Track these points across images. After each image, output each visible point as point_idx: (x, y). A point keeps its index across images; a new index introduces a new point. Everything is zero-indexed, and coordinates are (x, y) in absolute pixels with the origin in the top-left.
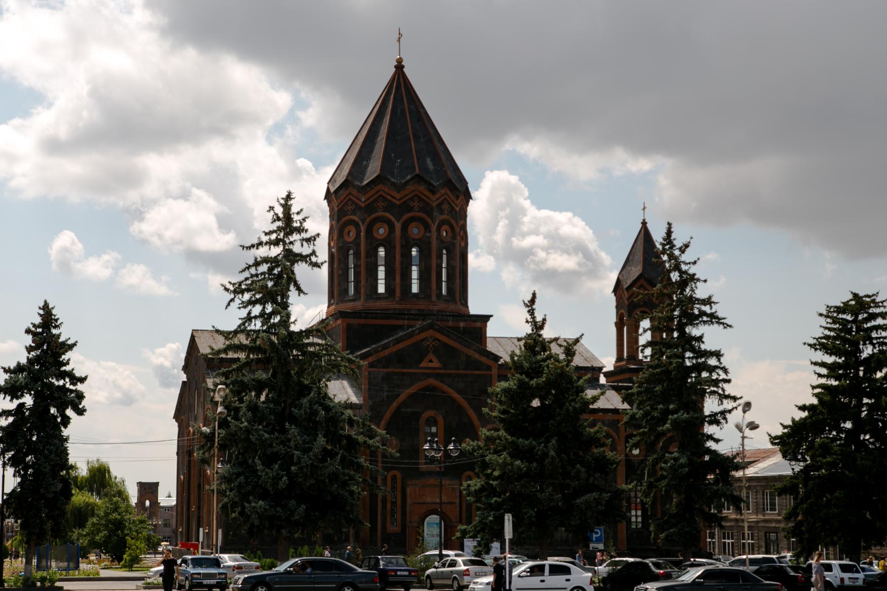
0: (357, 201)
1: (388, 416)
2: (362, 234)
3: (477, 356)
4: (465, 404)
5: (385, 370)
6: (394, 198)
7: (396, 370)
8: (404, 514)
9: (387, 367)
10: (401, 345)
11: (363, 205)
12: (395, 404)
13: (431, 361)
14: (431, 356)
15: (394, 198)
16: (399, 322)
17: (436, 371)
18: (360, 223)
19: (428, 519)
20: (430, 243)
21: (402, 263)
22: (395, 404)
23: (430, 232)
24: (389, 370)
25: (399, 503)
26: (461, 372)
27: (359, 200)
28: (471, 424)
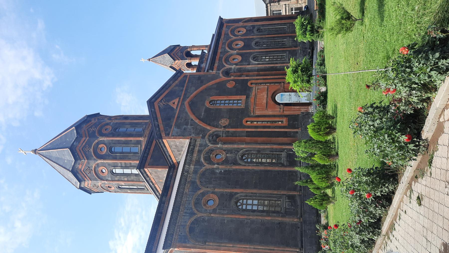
2: (102, 161)
3: (177, 82)
4: (204, 87)
5: (173, 127)
6: (85, 140)
7: (175, 121)
11: (86, 161)
12: (197, 121)
13: (174, 103)
14: (171, 104)
15: (85, 140)
19: (278, 101)
24: (173, 125)
26: (184, 89)
28: (218, 83)
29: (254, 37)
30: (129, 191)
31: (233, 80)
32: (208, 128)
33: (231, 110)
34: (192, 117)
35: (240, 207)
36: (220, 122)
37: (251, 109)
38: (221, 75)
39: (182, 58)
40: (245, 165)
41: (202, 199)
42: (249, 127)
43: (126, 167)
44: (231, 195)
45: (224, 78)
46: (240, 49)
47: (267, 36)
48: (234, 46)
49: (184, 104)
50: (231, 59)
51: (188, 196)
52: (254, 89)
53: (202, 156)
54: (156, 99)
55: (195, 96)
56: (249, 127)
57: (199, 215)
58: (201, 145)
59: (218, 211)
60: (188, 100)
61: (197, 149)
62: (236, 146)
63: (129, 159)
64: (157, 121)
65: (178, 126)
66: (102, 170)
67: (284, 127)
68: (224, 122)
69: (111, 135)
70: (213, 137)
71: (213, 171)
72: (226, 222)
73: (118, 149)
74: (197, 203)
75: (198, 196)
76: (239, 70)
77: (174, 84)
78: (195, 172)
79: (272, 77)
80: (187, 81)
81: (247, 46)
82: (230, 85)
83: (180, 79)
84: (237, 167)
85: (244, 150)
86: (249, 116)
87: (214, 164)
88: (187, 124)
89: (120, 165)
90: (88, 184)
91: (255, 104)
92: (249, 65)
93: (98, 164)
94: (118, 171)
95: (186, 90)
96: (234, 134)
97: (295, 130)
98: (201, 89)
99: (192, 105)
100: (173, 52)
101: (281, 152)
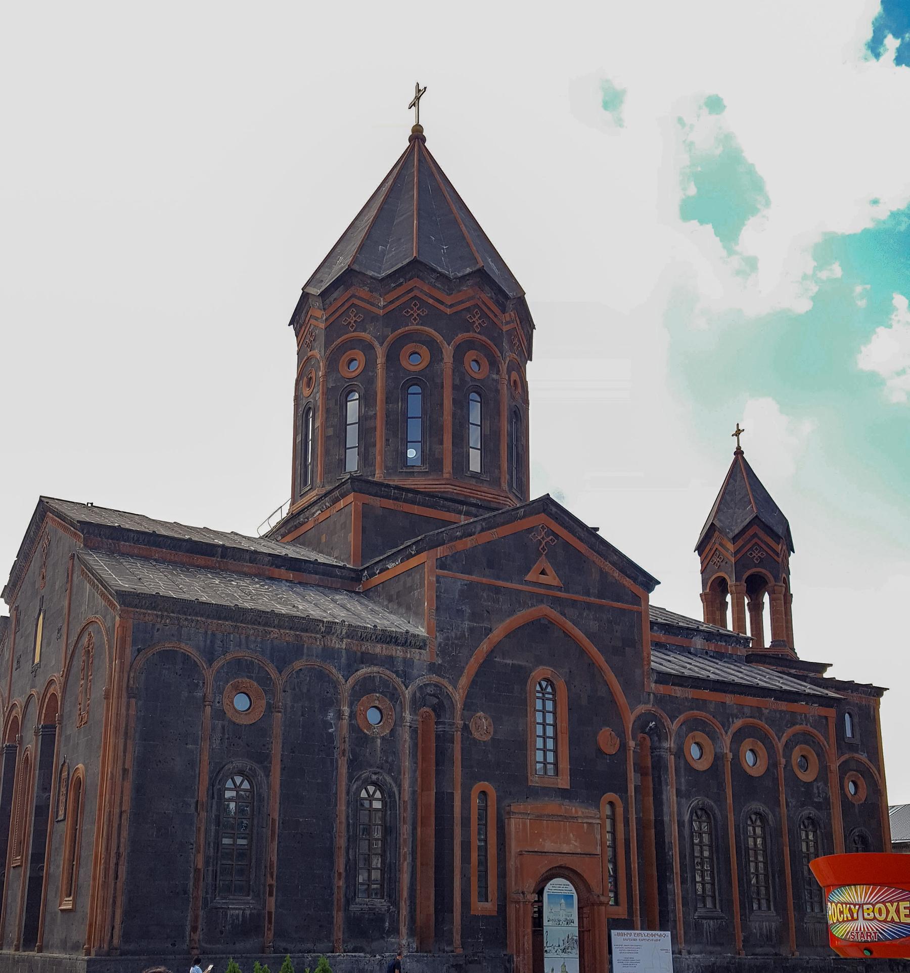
0: (368, 306)
1: (472, 666)
2: (380, 360)
3: (616, 574)
4: (601, 659)
7: (484, 580)
8: (502, 875)
9: (470, 573)
12: (484, 647)
13: (543, 573)
14: (543, 563)
17: (551, 592)
18: (376, 344)
20: (497, 391)
21: (454, 415)
23: (498, 372)
24: (474, 578)
25: (492, 851)
27: (372, 304)
28: (614, 702)
29: (784, 809)
30: (299, 439)
31: (623, 746)
32: (464, 681)
33: (519, 745)
34: (498, 632)
35: (229, 784)
36: (481, 714)
38: (641, 709)
39: (740, 566)
40: (348, 793)
41: (250, 677)
42: (466, 800)
43: (365, 432)
44: (263, 758)
45: (630, 719)
46: (737, 761)
47: (787, 850)
48: (747, 743)
49: (542, 601)
50: (700, 736)
51: (259, 639)
52: (592, 811)
53: (375, 669)
54: (555, 518)
55: (567, 634)
56: (466, 800)
57: (209, 674)
58: (408, 663)
59: (219, 724)
60: (554, 614)
61: (398, 652)
62: (407, 763)
63: (387, 440)
64: (483, 530)
65: (470, 592)
66: (353, 360)
67: (466, 904)
68: (483, 726)
69: (457, 382)
70: (434, 695)
71: (329, 702)
72: (189, 746)
73: (415, 405)
74: (241, 667)
75: (260, 667)
76: (659, 765)
77: (608, 567)
78: (329, 654)
79: (635, 866)
80: (619, 605)
81: (747, 786)
82: (606, 739)
83: (627, 582)
84: (344, 770)
85: (395, 789)
86: (499, 800)
87: (351, 705)
88: (474, 616)
89: (371, 413)
90: (316, 319)
91: (539, 817)
92: (679, 793)
93: (371, 347)
94: (353, 408)
95: (589, 606)
96: (442, 758)
97: (457, 938)
98: (593, 650)
99: (539, 629)
100: (761, 534)
101: (390, 896)
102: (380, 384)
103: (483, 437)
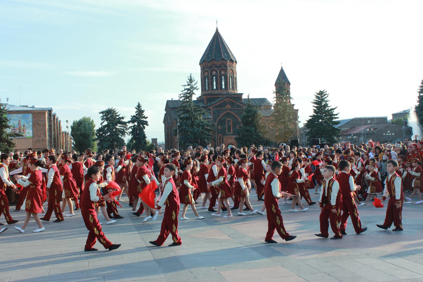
4: (237, 116)
10: (220, 102)
12: (219, 117)
14: (228, 105)
16: (219, 96)
22: (219, 117)
32: (217, 122)
34: (221, 115)
37: (226, 137)
42: (218, 137)
43: (208, 84)
55: (232, 114)
65: (217, 111)
68: (220, 127)
83: (242, 105)
95: (235, 109)
99: (228, 114)
102: (210, 77)
103: (225, 83)
